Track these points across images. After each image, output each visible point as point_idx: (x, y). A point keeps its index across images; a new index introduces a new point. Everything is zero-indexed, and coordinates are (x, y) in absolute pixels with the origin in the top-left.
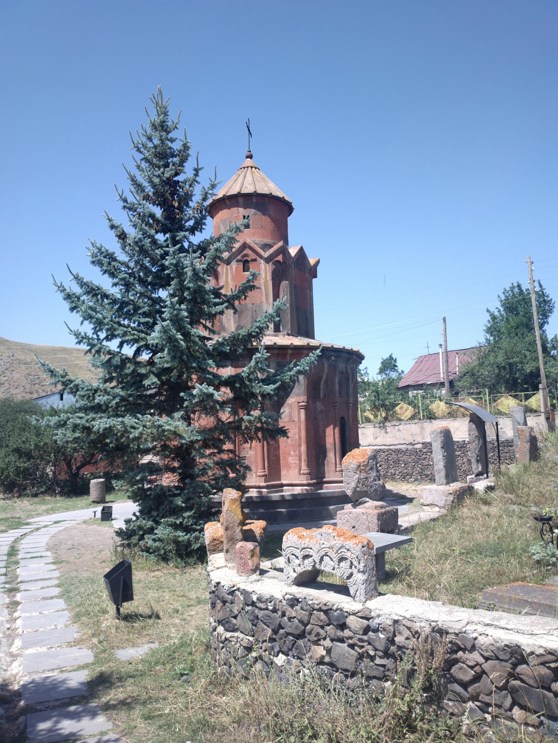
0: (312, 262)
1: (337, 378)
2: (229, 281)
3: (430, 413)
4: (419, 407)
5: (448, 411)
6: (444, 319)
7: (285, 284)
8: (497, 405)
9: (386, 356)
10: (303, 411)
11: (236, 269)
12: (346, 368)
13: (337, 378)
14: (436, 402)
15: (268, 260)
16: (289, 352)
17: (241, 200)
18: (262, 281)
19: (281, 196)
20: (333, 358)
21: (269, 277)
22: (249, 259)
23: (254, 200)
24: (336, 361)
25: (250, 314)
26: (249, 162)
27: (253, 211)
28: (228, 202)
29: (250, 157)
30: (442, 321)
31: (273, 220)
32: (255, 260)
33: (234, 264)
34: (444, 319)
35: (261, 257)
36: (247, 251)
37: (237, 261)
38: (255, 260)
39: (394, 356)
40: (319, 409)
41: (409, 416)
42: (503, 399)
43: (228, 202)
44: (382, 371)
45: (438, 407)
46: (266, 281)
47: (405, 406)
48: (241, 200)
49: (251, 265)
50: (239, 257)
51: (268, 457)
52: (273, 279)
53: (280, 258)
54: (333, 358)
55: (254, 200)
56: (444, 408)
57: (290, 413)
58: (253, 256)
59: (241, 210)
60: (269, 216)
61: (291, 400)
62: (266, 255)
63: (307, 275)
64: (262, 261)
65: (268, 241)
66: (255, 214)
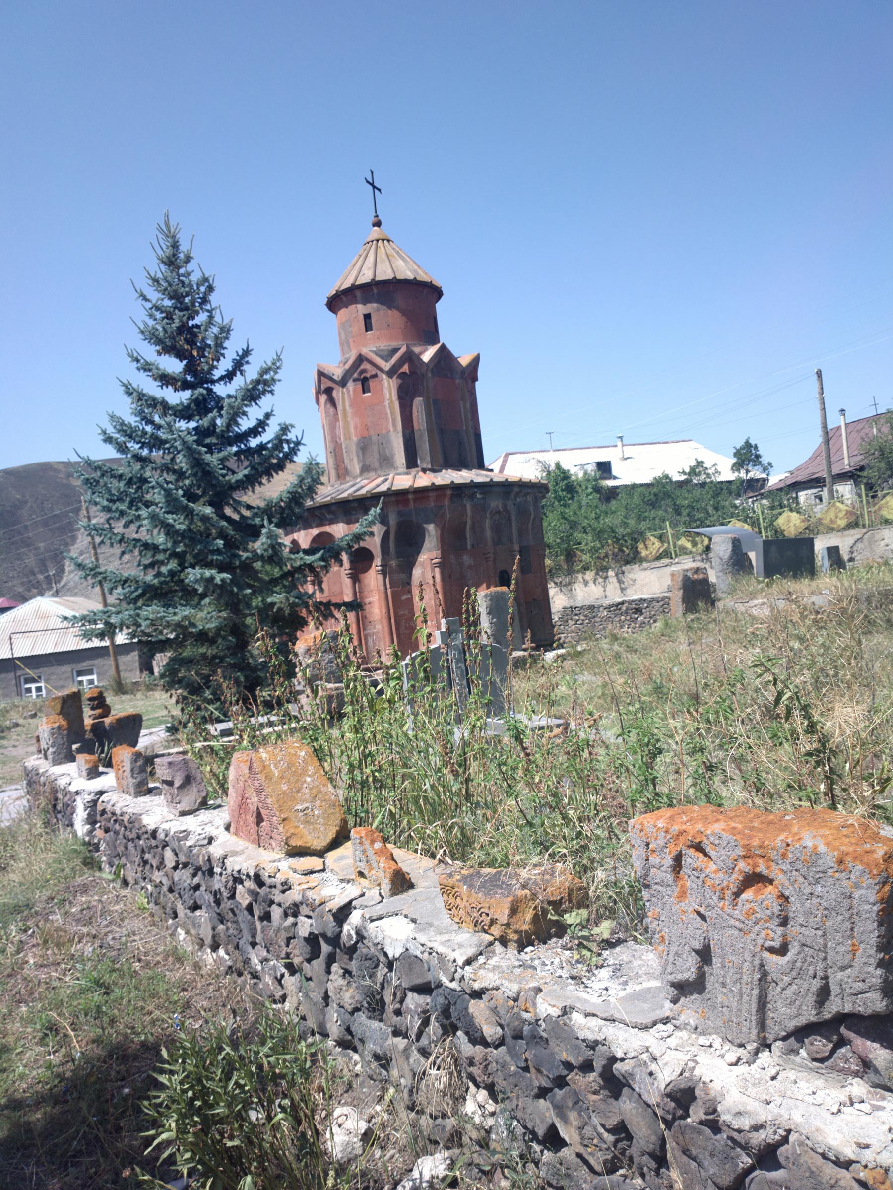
0: (464, 361)
1: (488, 521)
2: (347, 408)
3: (776, 532)
4: (759, 524)
6: (819, 374)
7: (418, 402)
8: (880, 509)
9: (740, 443)
10: (437, 570)
11: (354, 391)
12: (505, 506)
13: (488, 521)
14: (784, 515)
15: (391, 373)
16: (410, 496)
17: (358, 293)
18: (387, 403)
19: (410, 276)
20: (478, 496)
21: (395, 397)
22: (368, 375)
23: (375, 291)
24: (484, 498)
25: (375, 448)
26: (375, 232)
27: (375, 305)
28: (344, 299)
29: (378, 224)
30: (816, 377)
31: (404, 313)
32: (375, 376)
33: (351, 385)
34: (819, 374)
35: (382, 370)
36: (365, 366)
37: (355, 380)
38: (375, 376)
39: (753, 442)
40: (467, 564)
43: (344, 299)
44: (737, 467)
45: (789, 521)
46: (391, 402)
48: (358, 293)
49: (372, 383)
50: (355, 375)
51: (397, 630)
52: (400, 398)
53: (406, 368)
54: (478, 496)
55: (375, 291)
56: (798, 521)
57: (423, 573)
58: (372, 370)
59: (360, 306)
60: (398, 309)
61: (423, 557)
62: (387, 366)
63: (457, 381)
64: (384, 376)
65: (394, 344)
66: (378, 310)
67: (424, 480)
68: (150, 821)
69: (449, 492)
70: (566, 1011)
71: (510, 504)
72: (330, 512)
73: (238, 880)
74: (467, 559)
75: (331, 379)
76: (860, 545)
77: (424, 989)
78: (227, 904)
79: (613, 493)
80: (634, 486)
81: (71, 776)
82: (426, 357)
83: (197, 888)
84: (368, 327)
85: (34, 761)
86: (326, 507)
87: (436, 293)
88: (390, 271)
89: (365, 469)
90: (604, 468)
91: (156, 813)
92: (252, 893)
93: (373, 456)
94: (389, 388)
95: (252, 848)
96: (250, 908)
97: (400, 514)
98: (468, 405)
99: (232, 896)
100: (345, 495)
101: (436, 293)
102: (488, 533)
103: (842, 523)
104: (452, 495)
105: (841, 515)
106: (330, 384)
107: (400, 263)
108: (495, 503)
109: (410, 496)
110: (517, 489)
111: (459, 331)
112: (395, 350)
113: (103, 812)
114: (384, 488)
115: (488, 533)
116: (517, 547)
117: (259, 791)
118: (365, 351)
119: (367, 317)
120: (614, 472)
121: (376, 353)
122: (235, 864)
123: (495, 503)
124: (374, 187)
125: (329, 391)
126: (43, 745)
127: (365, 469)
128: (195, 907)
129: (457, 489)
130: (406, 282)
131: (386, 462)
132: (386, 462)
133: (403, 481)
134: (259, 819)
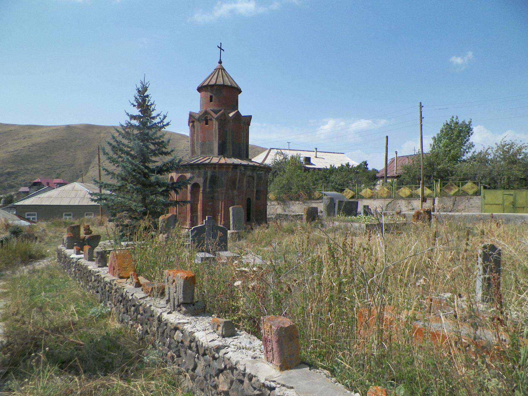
5: (371, 194)
6: (387, 137)
12: (252, 174)
13: (245, 179)
21: (217, 128)
30: (385, 139)
34: (387, 137)
41: (350, 196)
42: (402, 189)
45: (366, 192)
46: (215, 130)
47: (349, 190)
48: (209, 88)
49: (209, 122)
56: (370, 193)
62: (215, 116)
63: (242, 125)
67: (223, 161)
68: (90, 268)
69: (232, 166)
70: (151, 306)
71: (255, 174)
72: (186, 168)
73: (106, 284)
74: (235, 192)
75: (194, 118)
76: (390, 205)
77: (134, 306)
78: (104, 290)
79: (307, 170)
80: (319, 169)
81: (72, 254)
82: (231, 115)
83: (98, 287)
84: (211, 101)
85: (60, 247)
86: (185, 165)
87: (240, 91)
88: (222, 81)
89: (202, 153)
90: (308, 160)
91: (92, 266)
92: (109, 287)
93: (206, 150)
94: (215, 125)
95: (112, 276)
96: (108, 291)
97: (212, 172)
98: (245, 134)
99: (105, 288)
100: (192, 162)
101: (240, 91)
102: (245, 183)
103: (385, 195)
104: (233, 168)
105: (385, 192)
106: (194, 120)
107: (226, 79)
108: (249, 173)
109: (217, 166)
110: (258, 168)
111: (244, 107)
112: (220, 111)
113: (78, 265)
114: (207, 162)
115: (245, 183)
116: (255, 190)
117: (115, 261)
118: (209, 109)
119: (211, 97)
120: (312, 161)
121: (212, 110)
122: (107, 279)
123: (249, 173)
124: (221, 49)
125: (193, 122)
126: (65, 242)
127: (202, 153)
128: (98, 292)
129: (236, 166)
130: (227, 86)
131: (211, 151)
132: (211, 151)
133: (215, 160)
134: (114, 269)
